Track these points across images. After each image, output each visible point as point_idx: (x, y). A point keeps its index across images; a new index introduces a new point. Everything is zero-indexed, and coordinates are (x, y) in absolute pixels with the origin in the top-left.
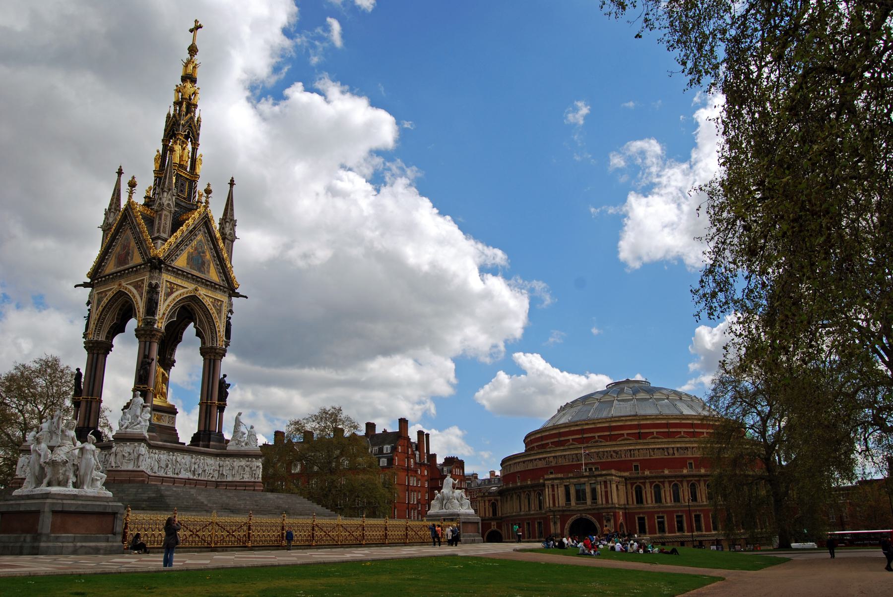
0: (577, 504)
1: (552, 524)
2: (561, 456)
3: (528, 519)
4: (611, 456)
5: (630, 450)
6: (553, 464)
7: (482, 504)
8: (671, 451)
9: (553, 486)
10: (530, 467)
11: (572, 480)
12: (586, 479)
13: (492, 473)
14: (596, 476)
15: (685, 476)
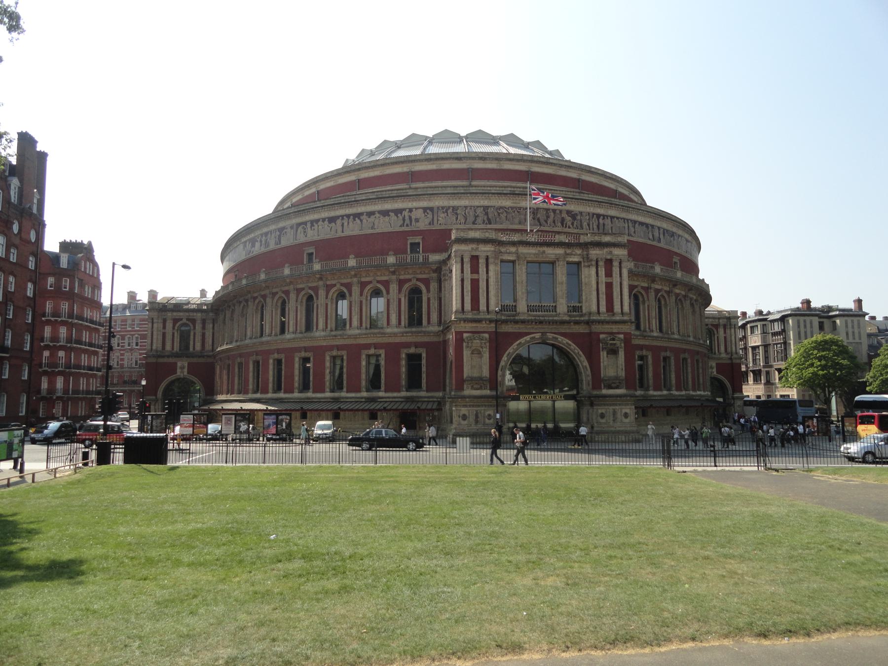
0: (530, 309)
1: (466, 353)
2: (445, 209)
3: (339, 348)
4: (563, 221)
5: (598, 216)
6: (423, 225)
7: (158, 326)
8: (656, 234)
9: (475, 259)
10: (353, 229)
11: (523, 250)
12: (560, 251)
13: (132, 296)
14: (585, 246)
15: (675, 283)
